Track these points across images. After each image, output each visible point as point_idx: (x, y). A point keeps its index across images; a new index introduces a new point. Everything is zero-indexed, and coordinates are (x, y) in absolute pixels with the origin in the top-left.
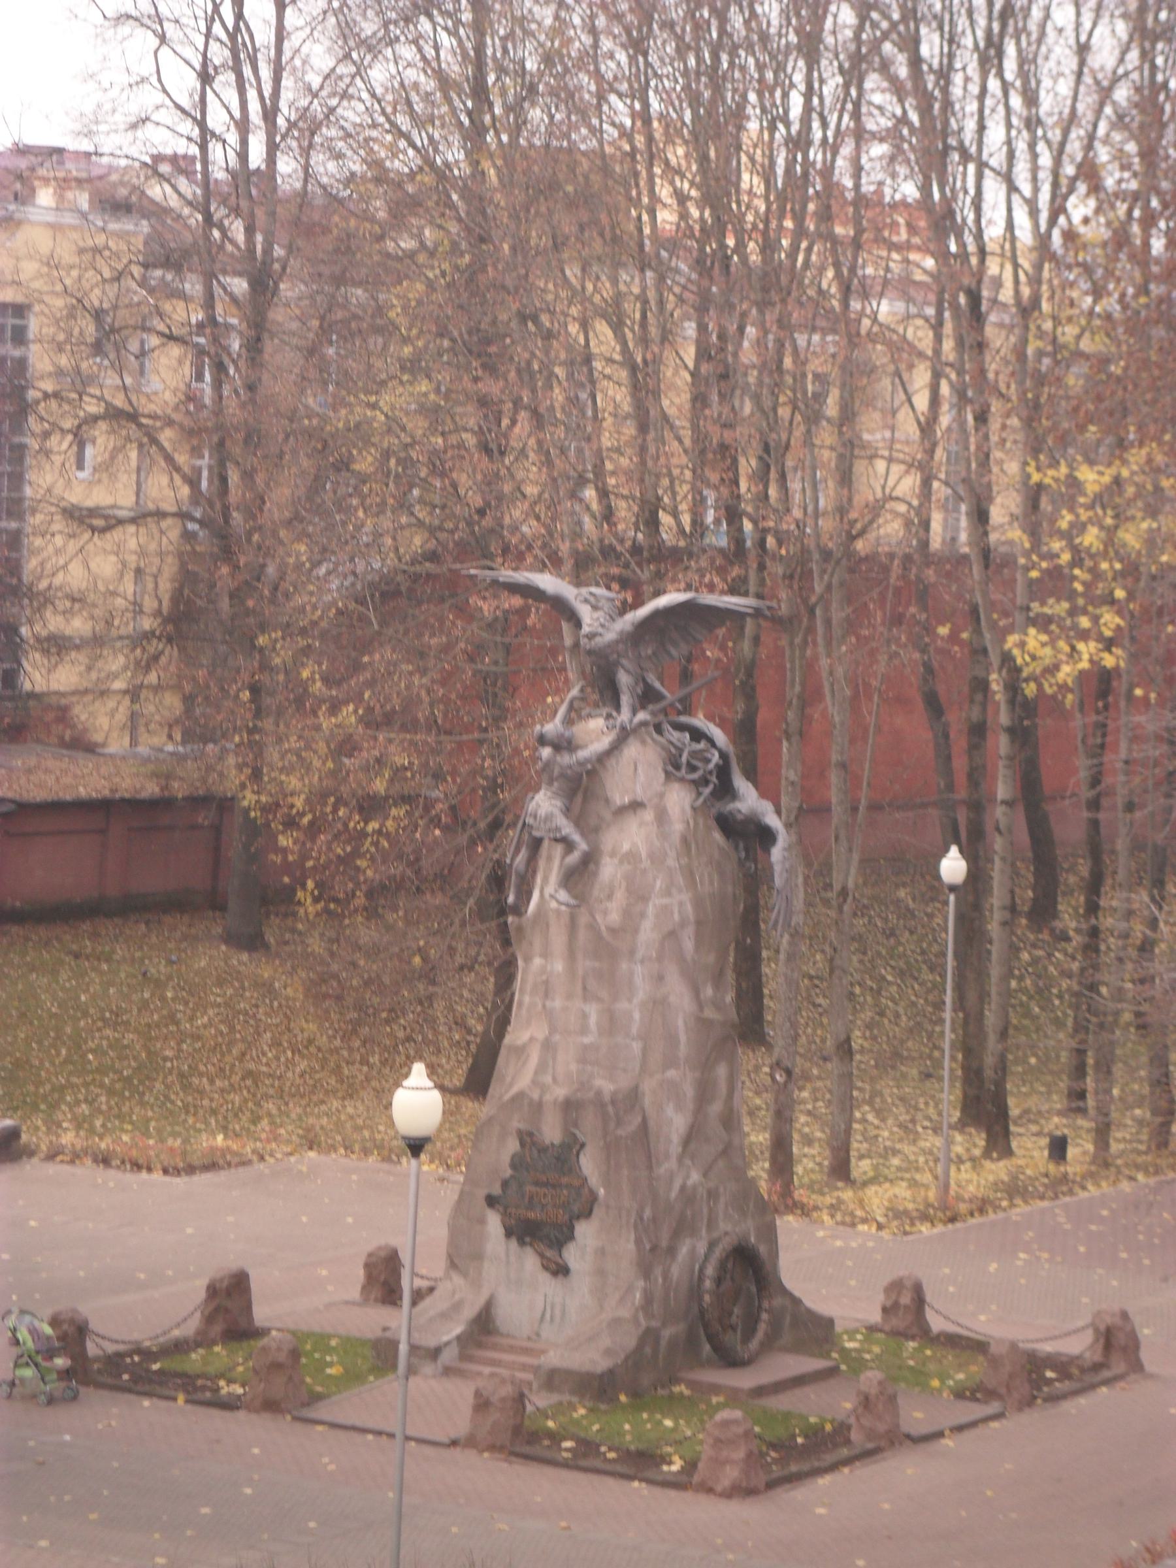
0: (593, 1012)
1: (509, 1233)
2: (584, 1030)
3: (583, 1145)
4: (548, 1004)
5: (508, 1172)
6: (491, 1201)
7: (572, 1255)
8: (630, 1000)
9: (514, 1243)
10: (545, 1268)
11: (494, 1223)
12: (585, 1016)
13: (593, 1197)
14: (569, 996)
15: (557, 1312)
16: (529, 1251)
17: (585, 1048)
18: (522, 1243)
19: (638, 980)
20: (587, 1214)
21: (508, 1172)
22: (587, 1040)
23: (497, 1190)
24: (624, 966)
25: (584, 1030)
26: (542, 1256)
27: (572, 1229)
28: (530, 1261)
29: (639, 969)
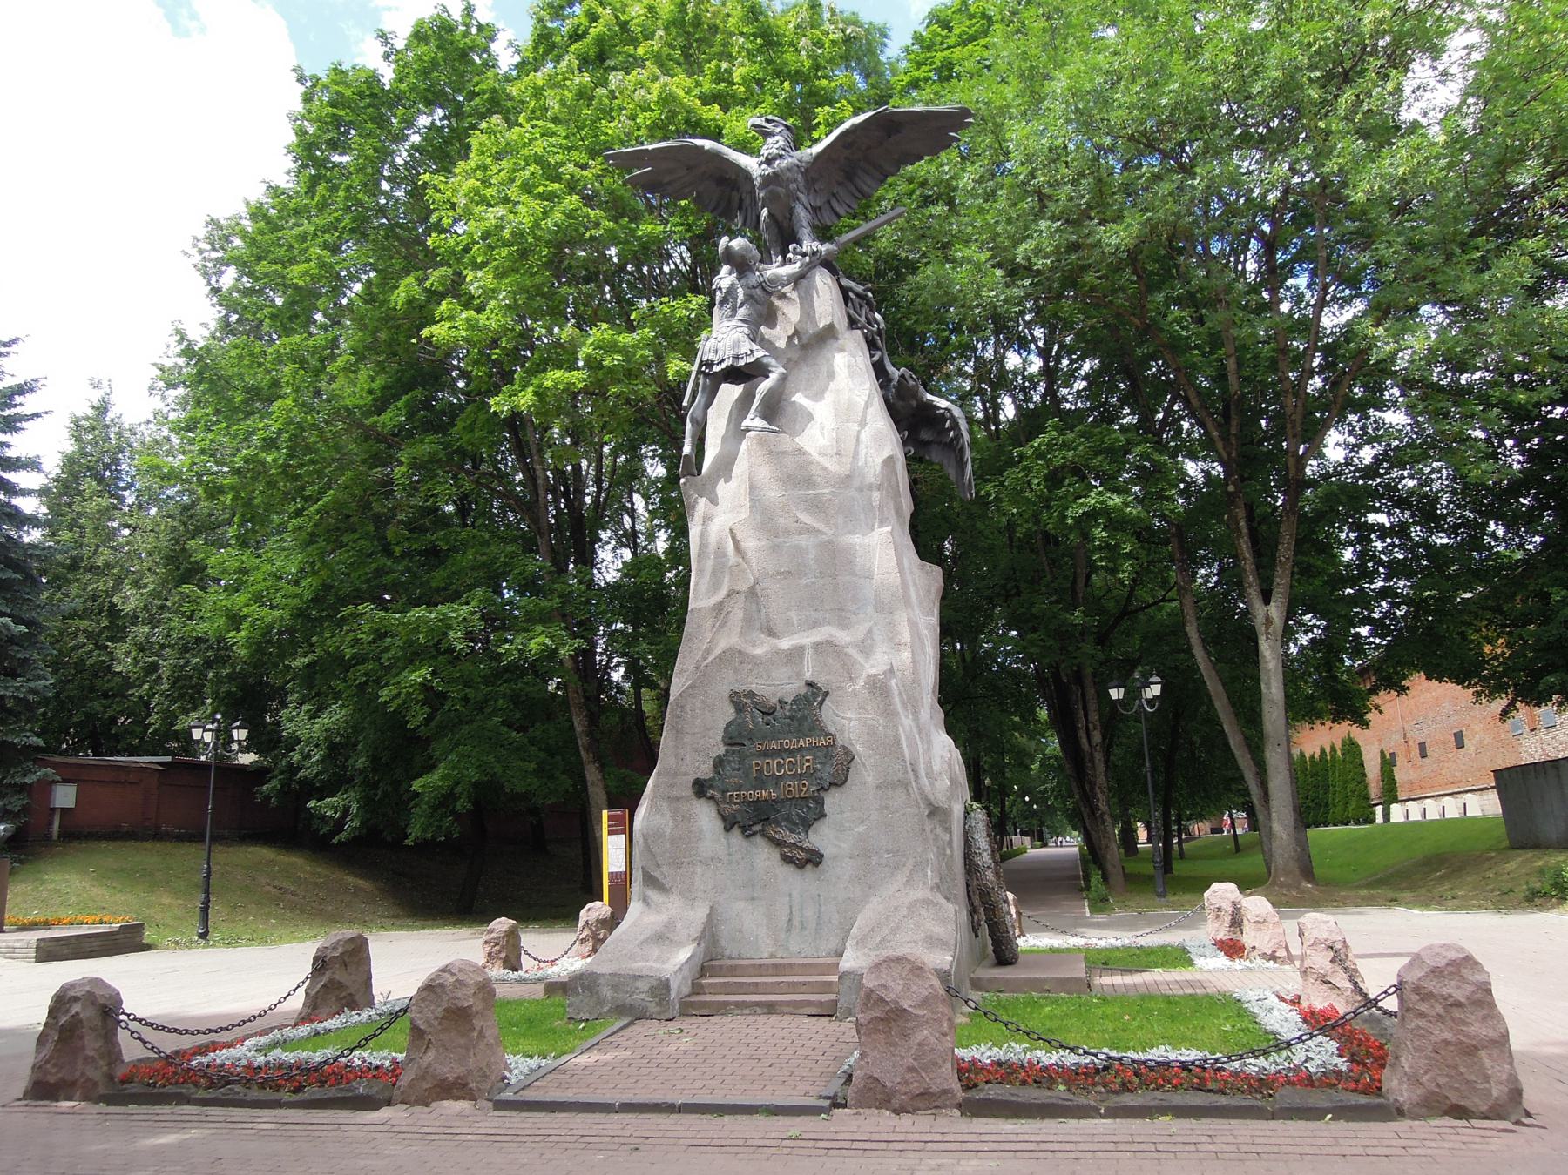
1: (729, 824)
3: (827, 694)
5: (722, 750)
6: (701, 788)
7: (821, 838)
9: (736, 831)
10: (788, 860)
11: (705, 817)
13: (849, 757)
16: (758, 839)
18: (747, 833)
20: (839, 782)
21: (722, 750)
23: (705, 770)
26: (777, 843)
28: (763, 856)
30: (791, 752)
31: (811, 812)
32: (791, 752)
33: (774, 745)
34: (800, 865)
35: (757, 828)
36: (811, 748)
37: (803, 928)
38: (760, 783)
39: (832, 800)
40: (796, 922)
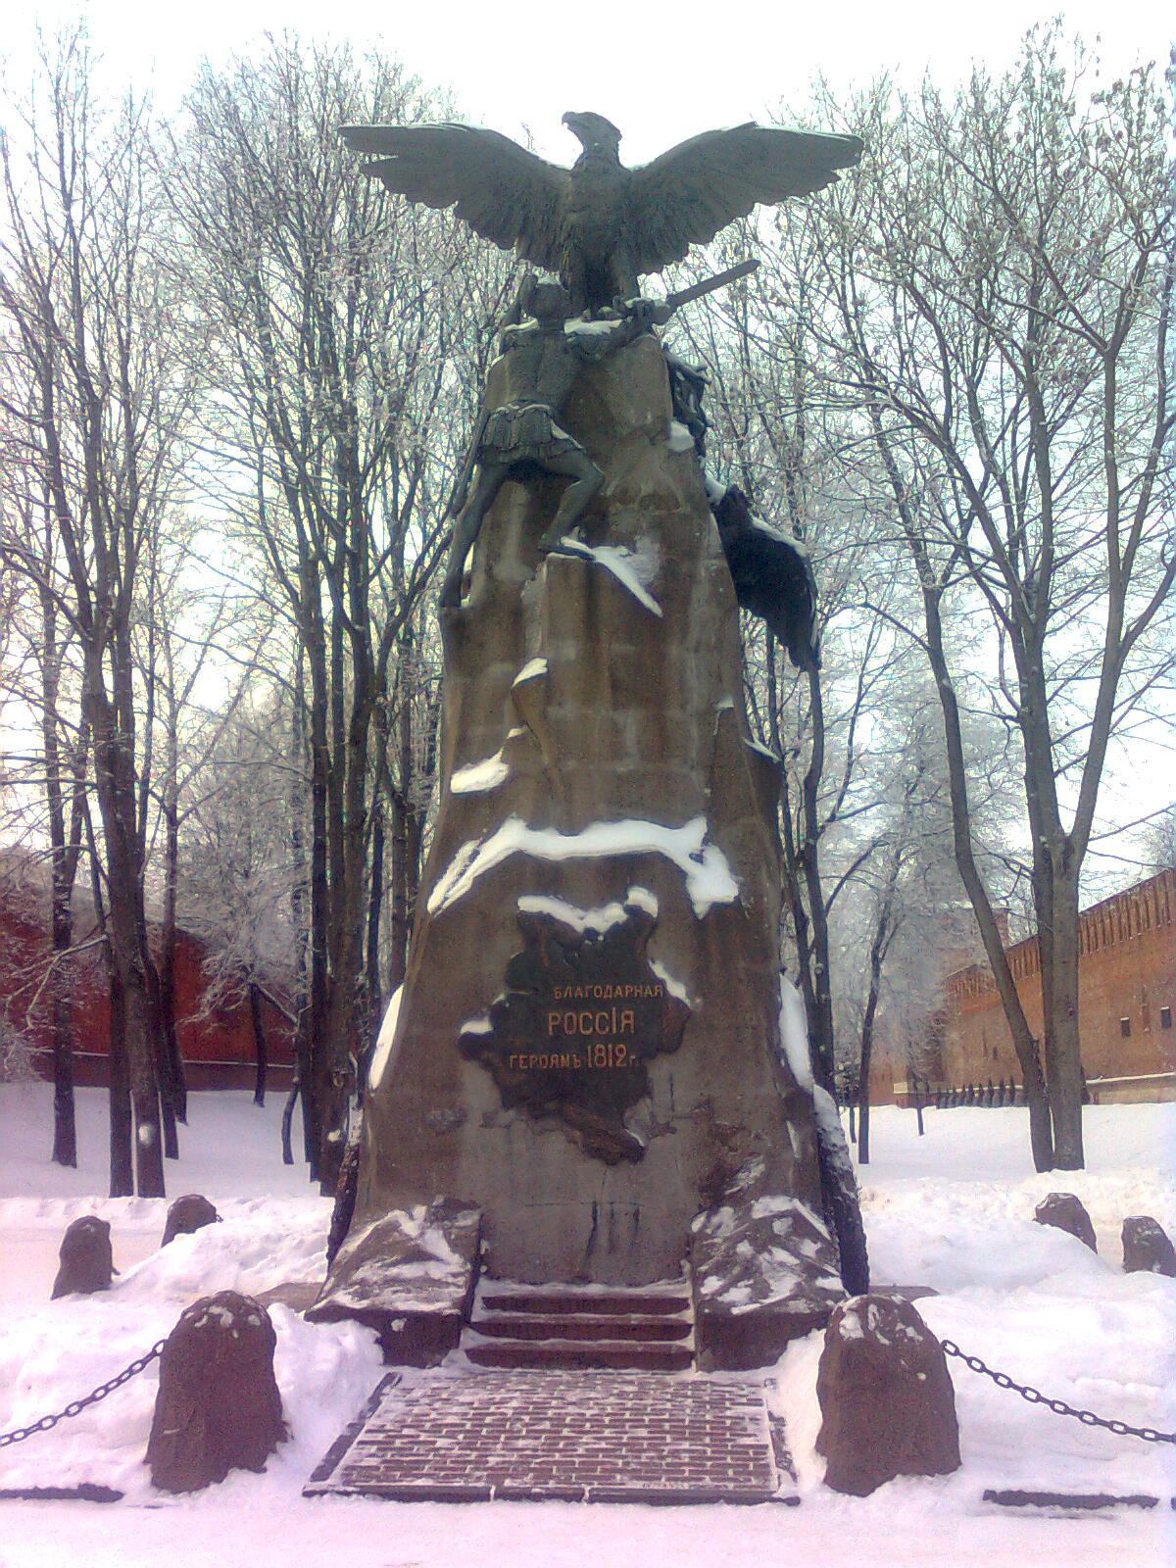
0: (631, 722)
1: (511, 1097)
2: (617, 752)
4: (554, 712)
8: (683, 707)
12: (616, 730)
14: (588, 698)
15: (623, 1227)
16: (551, 1123)
17: (621, 779)
19: (692, 681)
22: (621, 769)
24: (674, 650)
25: (617, 752)
27: (642, 1073)
28: (557, 1146)
29: (692, 661)
30: (605, 1005)
31: (634, 1087)
32: (605, 1005)
33: (579, 992)
34: (611, 1162)
35: (552, 1106)
36: (632, 1001)
37: (613, 1248)
38: (558, 1043)
39: (660, 1071)
40: (603, 1240)
